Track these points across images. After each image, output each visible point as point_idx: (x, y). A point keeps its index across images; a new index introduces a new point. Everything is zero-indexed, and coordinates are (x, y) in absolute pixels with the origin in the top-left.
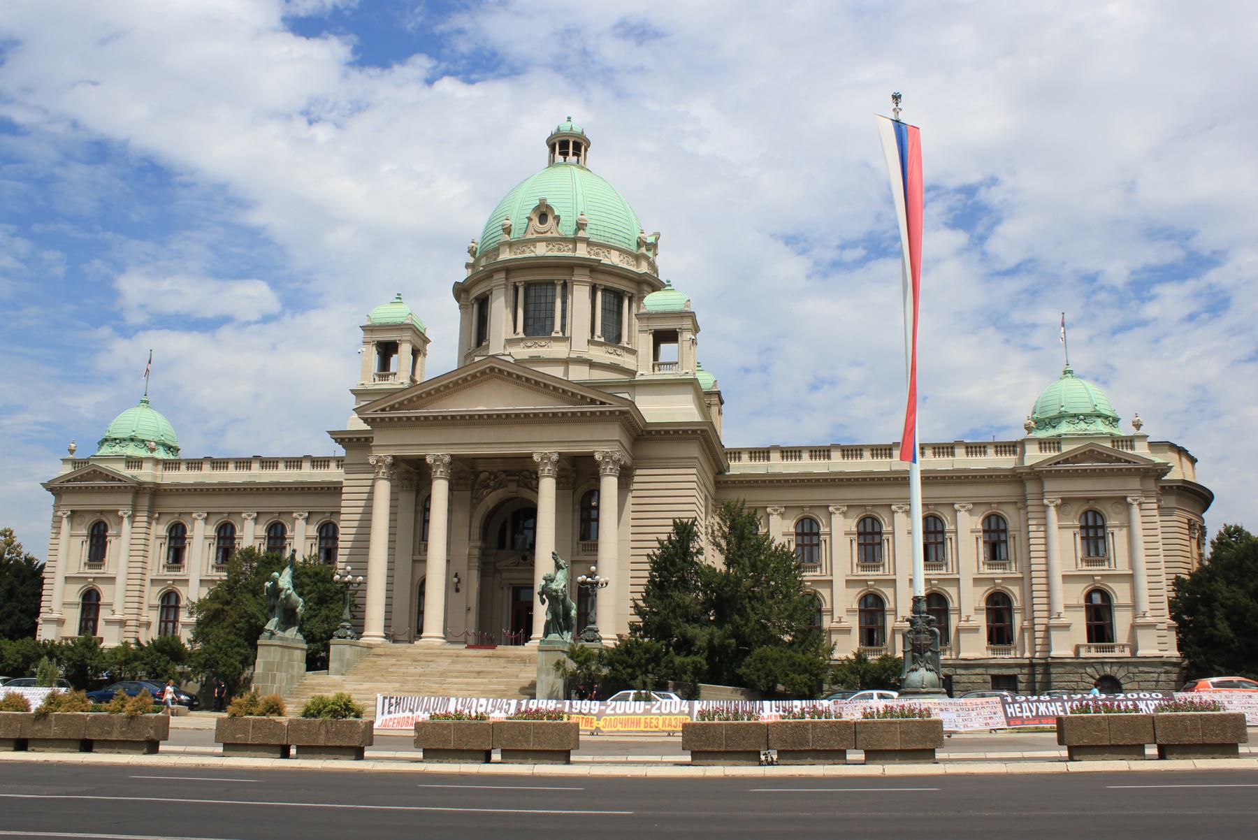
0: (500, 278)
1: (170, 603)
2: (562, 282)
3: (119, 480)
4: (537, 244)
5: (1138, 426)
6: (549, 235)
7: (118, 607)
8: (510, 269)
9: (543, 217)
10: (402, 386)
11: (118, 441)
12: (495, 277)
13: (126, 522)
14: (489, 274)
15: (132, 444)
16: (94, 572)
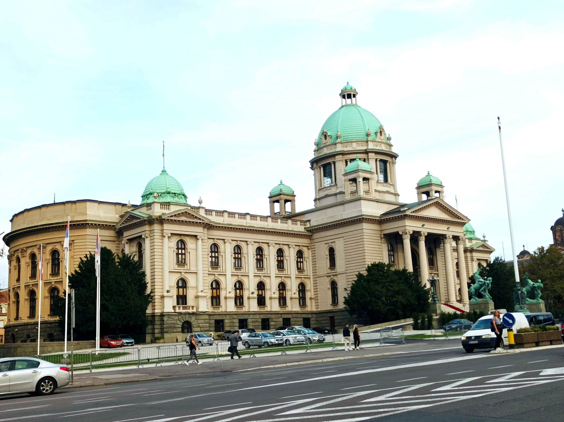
0: (371, 155)
1: (216, 286)
2: (389, 162)
3: (200, 219)
4: (382, 144)
5: (484, 237)
6: (383, 141)
7: (201, 288)
8: (377, 153)
9: (381, 132)
10: (375, 198)
11: (176, 195)
12: (370, 154)
13: (200, 242)
14: (366, 152)
15: (183, 197)
16: (181, 269)
